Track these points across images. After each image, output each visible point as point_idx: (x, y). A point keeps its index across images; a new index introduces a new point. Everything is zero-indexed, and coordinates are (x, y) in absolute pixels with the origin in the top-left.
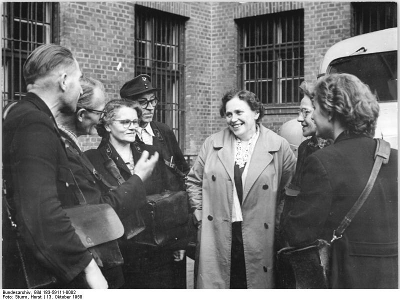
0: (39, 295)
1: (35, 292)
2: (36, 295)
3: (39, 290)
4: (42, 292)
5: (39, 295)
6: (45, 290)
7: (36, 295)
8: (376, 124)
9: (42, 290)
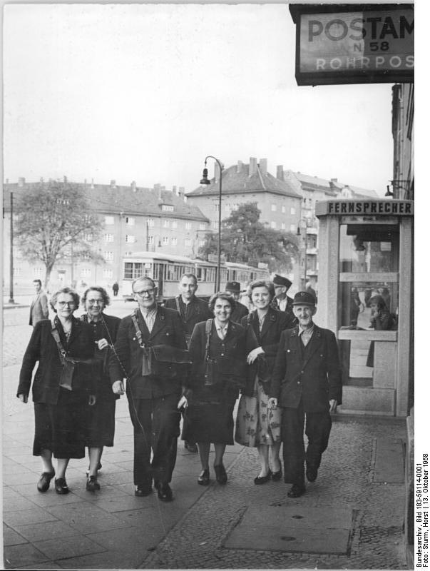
0: (423, 515)
1: (419, 521)
2: (423, 519)
3: (416, 515)
4: (419, 511)
5: (423, 515)
6: (415, 506)
7: (423, 519)
8: (54, 178)
9: (416, 510)
